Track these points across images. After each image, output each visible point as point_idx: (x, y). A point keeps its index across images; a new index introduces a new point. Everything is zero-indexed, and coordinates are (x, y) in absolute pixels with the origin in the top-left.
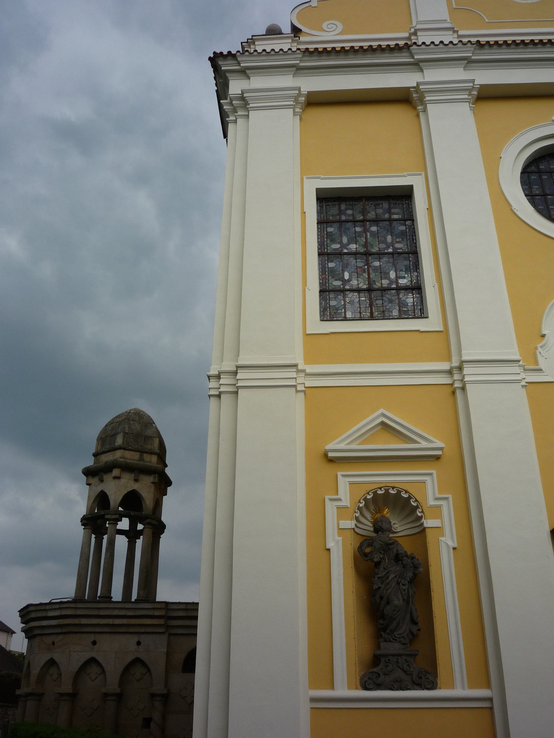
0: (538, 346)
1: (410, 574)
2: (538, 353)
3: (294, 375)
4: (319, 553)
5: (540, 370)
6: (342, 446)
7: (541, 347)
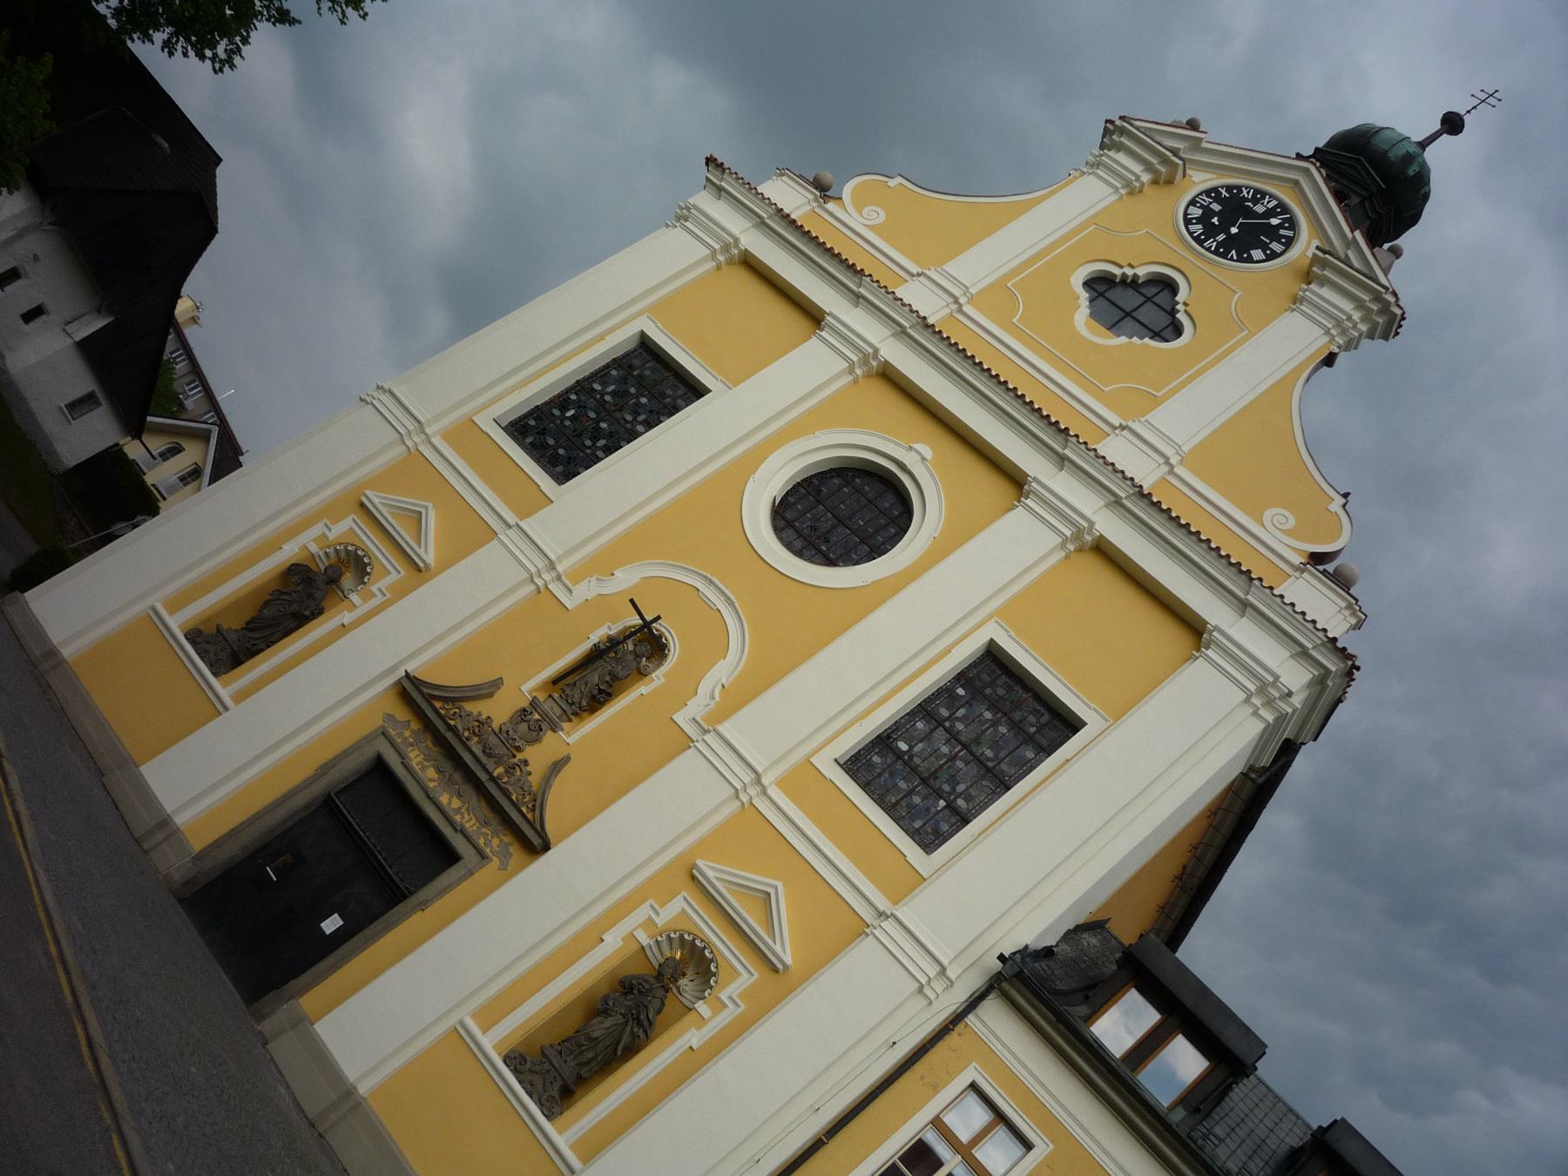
1: (295, 607)
3: (411, 427)
4: (275, 544)
6: (376, 501)
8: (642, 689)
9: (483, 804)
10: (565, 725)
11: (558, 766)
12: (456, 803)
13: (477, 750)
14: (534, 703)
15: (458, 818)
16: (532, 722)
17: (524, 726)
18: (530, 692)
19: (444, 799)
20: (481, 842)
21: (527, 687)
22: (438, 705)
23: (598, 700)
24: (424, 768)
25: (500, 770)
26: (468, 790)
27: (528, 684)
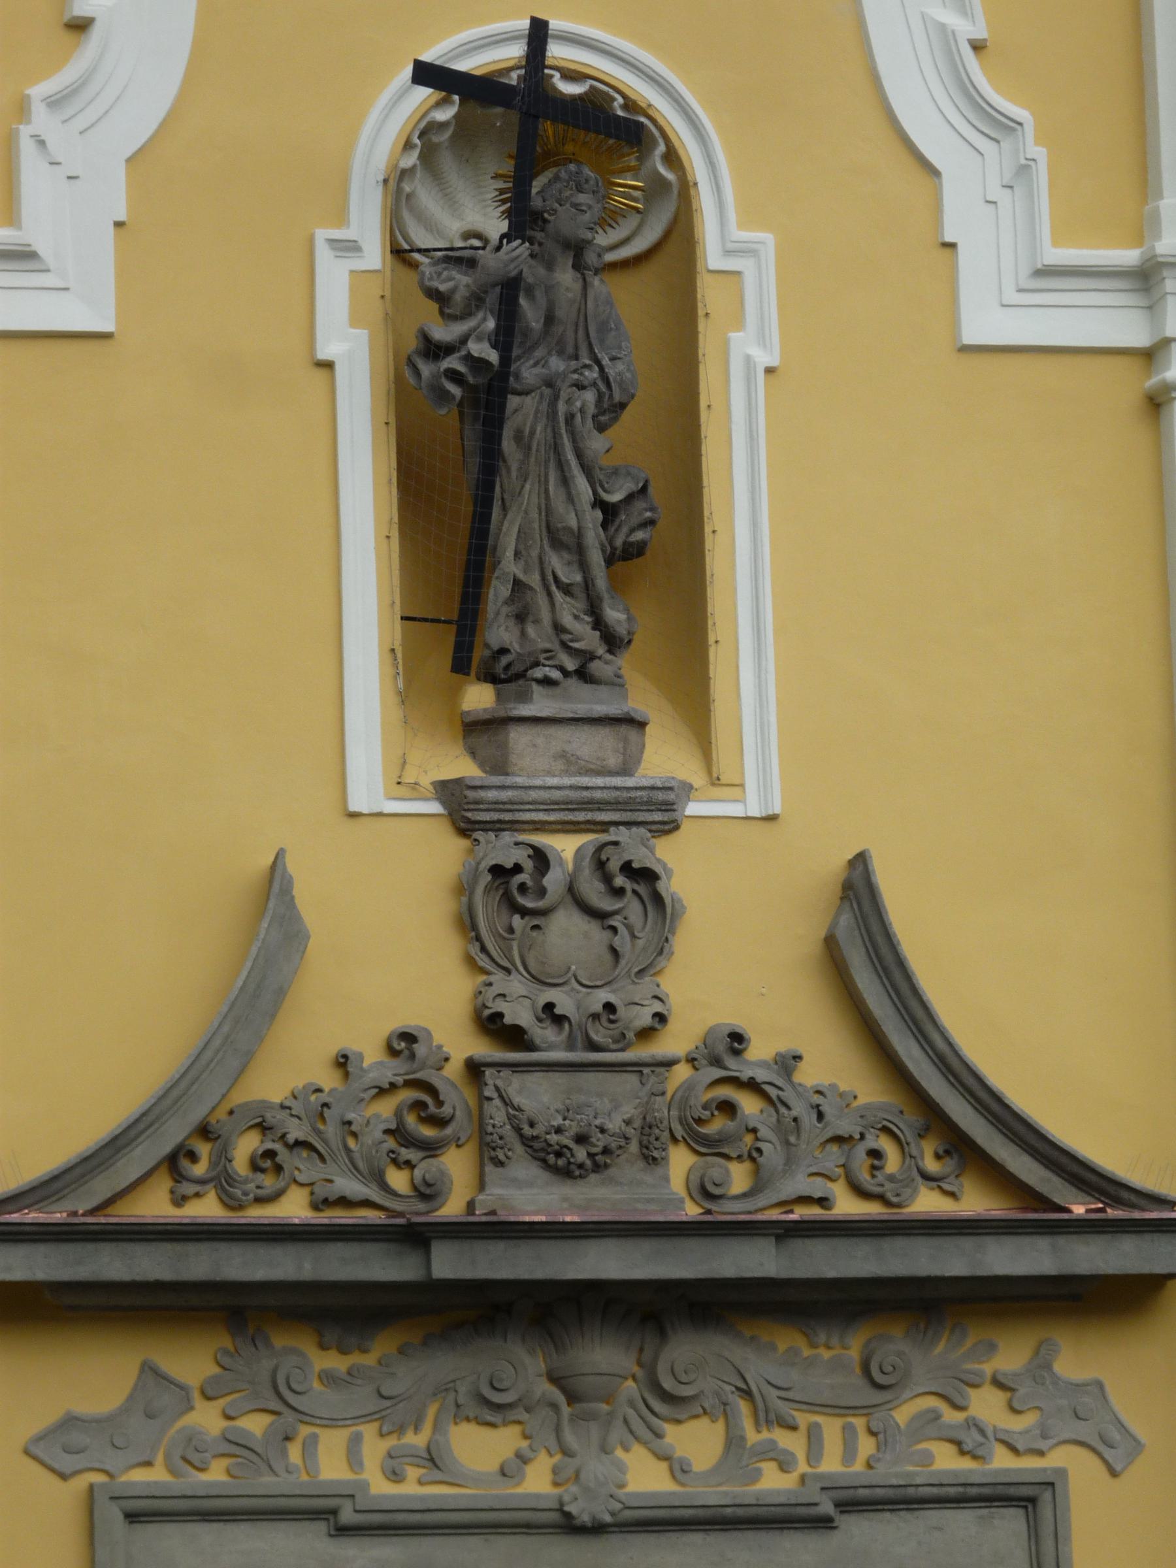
0: (38, 91)
2: (27, 147)
5: (24, 256)
7: (55, 103)
8: (744, 349)
9: (787, 1339)
10: (663, 757)
11: (859, 946)
12: (698, 1441)
13: (532, 1196)
14: (463, 811)
15: (773, 1482)
16: (555, 885)
17: (568, 936)
18: (400, 785)
19: (644, 1477)
20: (947, 1461)
21: (367, 788)
22: (154, 1205)
23: (650, 543)
24: (432, 1459)
25: (680, 1162)
26: (687, 1353)
27: (360, 759)
